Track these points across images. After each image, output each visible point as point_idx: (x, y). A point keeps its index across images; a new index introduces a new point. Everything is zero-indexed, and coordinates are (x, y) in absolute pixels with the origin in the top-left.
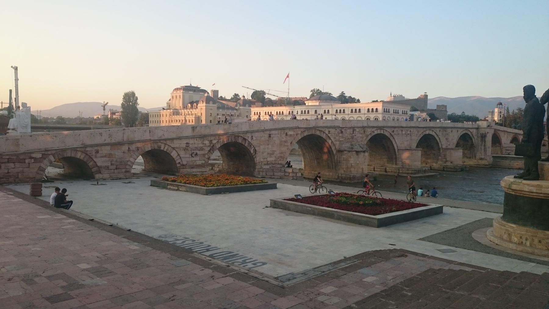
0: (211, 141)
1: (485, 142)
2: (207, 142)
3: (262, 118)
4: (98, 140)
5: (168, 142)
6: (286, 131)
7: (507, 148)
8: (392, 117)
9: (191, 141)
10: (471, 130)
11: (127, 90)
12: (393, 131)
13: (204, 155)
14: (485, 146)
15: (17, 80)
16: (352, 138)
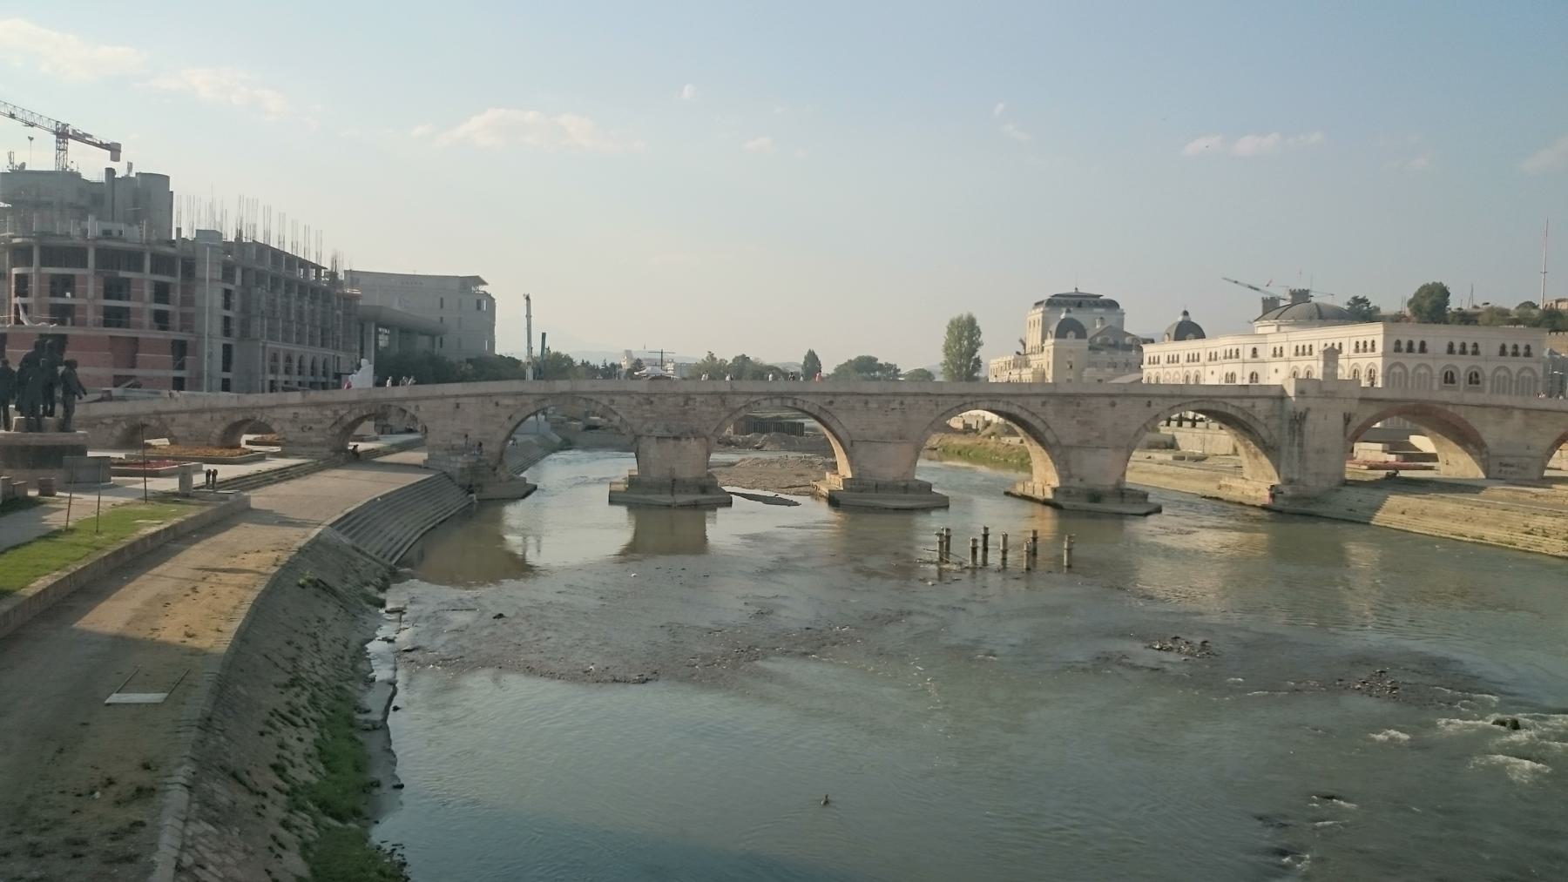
0: (336, 412)
1: (1302, 435)
2: (329, 413)
3: (1344, 372)
4: (173, 406)
5: (266, 411)
6: (495, 399)
7: (1507, 460)
8: (1438, 367)
9: (302, 411)
10: (1246, 403)
11: (961, 312)
12: (831, 403)
13: (324, 430)
14: (1301, 445)
15: (529, 316)
16: (685, 413)
